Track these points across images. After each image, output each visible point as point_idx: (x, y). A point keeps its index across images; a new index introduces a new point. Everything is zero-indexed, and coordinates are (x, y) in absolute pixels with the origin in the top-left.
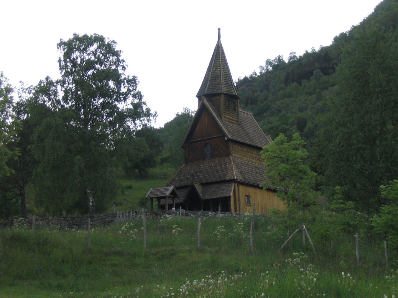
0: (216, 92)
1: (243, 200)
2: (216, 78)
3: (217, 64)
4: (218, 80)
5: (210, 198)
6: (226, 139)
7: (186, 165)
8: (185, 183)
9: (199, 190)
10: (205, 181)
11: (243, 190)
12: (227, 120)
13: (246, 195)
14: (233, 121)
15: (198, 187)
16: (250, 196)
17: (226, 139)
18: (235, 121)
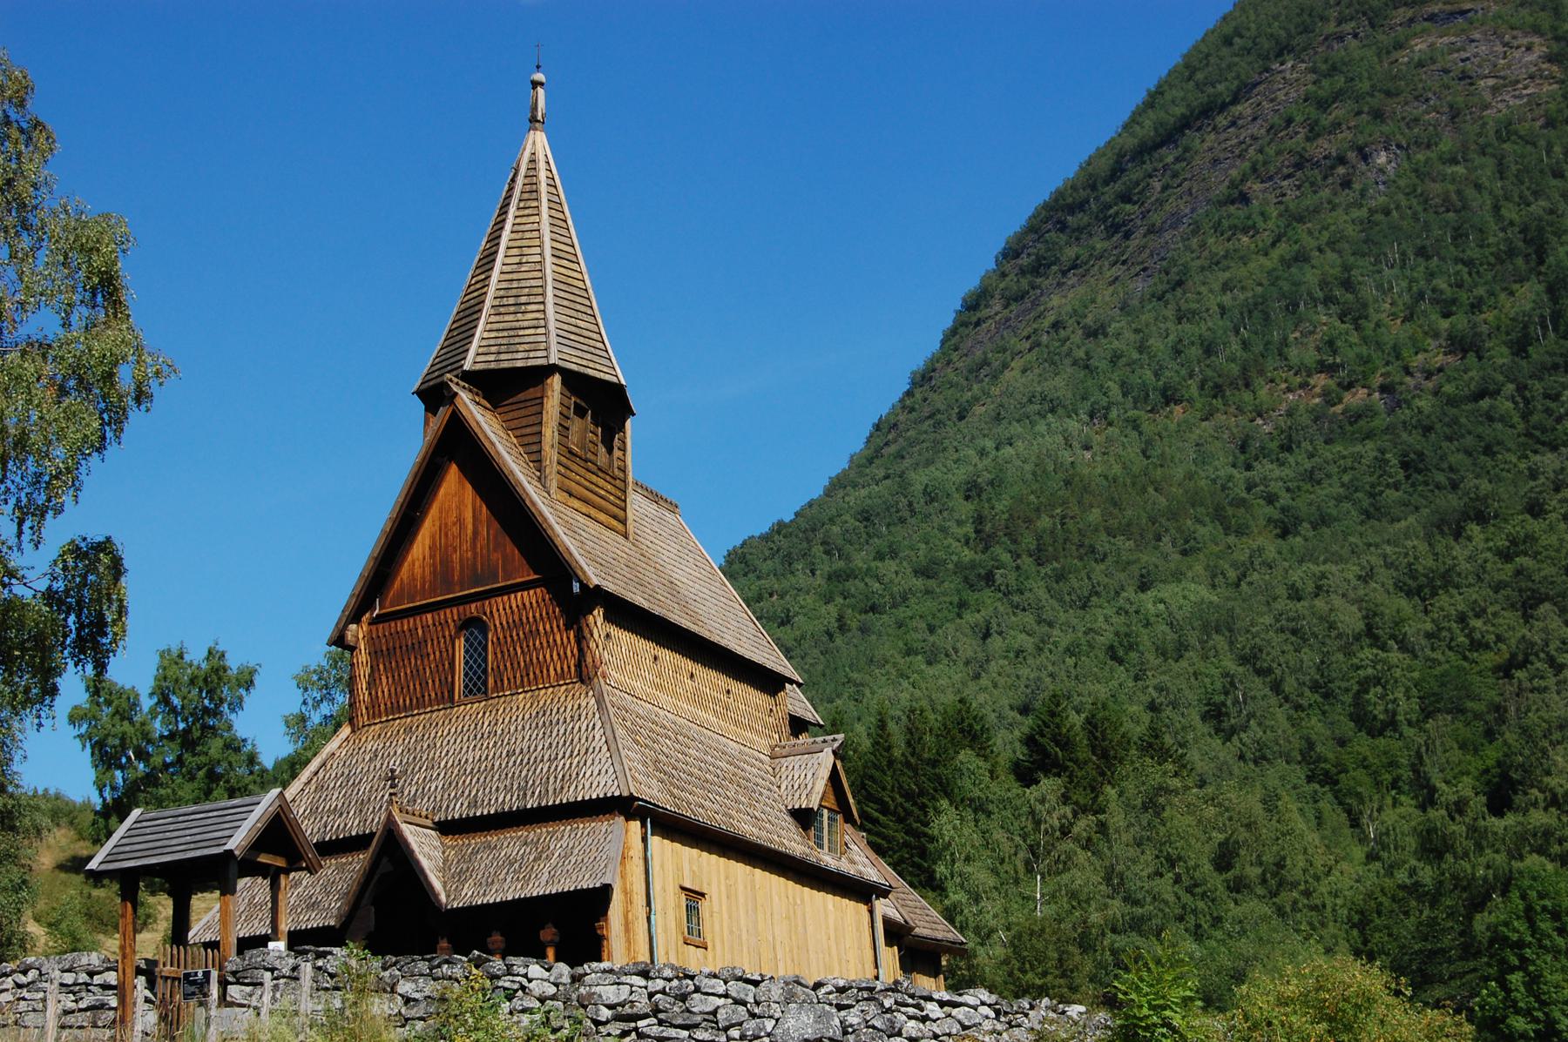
0: (519, 364)
1: (669, 908)
2: (523, 300)
3: (528, 235)
4: (530, 308)
5: (490, 899)
6: (576, 588)
7: (353, 731)
8: (353, 826)
9: (430, 858)
10: (459, 811)
11: (677, 862)
12: (577, 504)
13: (683, 888)
14: (602, 517)
15: (426, 848)
16: (703, 895)
17: (576, 588)
18: (615, 517)
